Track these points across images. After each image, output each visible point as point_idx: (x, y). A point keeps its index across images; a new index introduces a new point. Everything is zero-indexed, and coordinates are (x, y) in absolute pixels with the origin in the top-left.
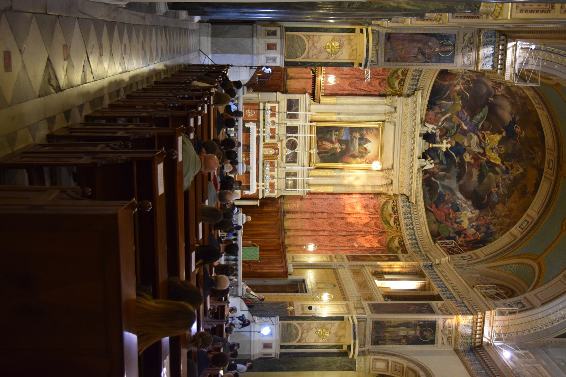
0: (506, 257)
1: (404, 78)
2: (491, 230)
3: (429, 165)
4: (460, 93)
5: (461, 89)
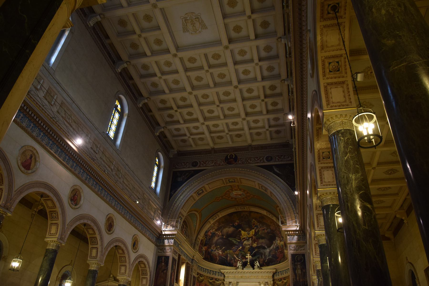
3: (257, 264)
4: (223, 251)
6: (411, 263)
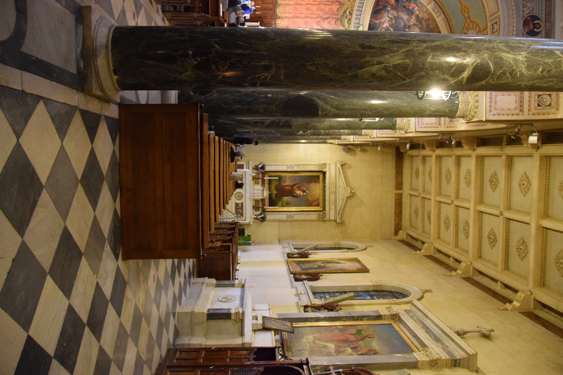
6: (366, 249)
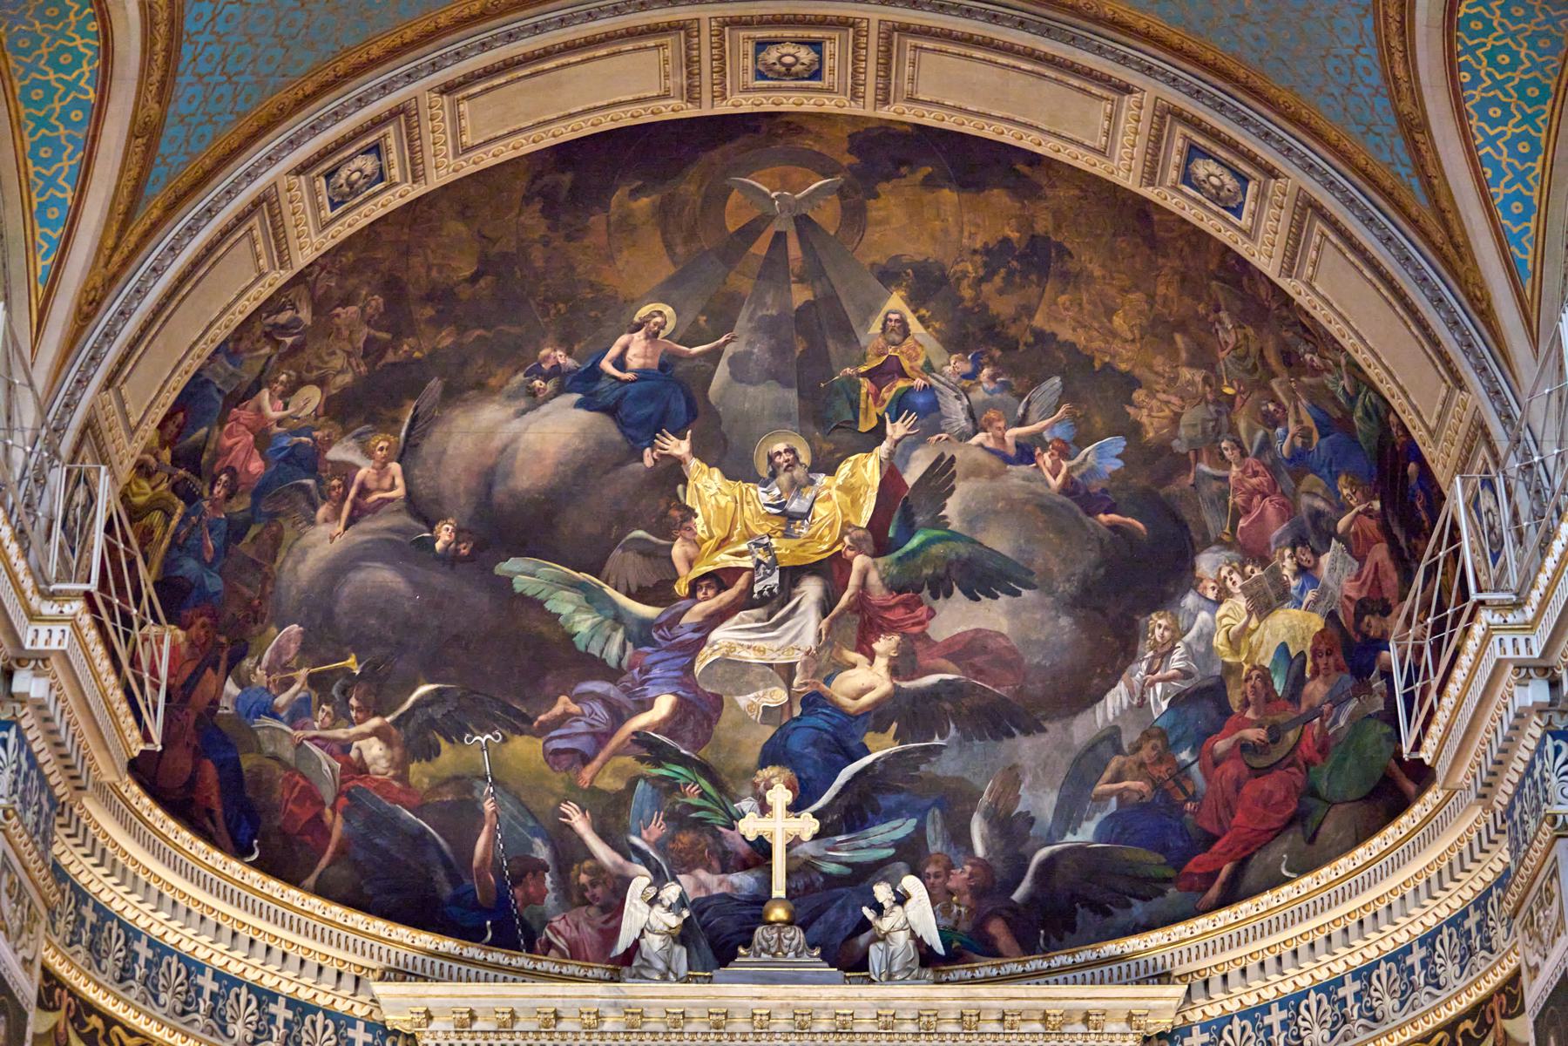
0: (1438, 237)
1: (67, 1000)
2: (1306, 434)
5: (376, 732)
